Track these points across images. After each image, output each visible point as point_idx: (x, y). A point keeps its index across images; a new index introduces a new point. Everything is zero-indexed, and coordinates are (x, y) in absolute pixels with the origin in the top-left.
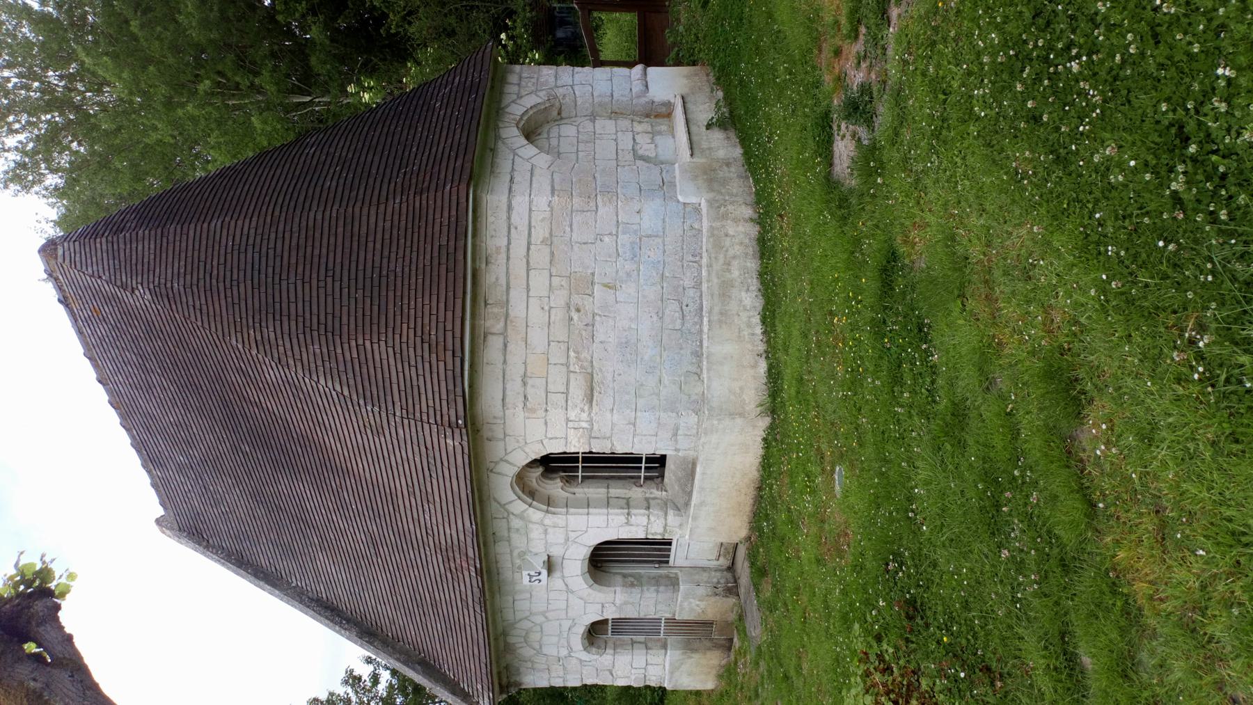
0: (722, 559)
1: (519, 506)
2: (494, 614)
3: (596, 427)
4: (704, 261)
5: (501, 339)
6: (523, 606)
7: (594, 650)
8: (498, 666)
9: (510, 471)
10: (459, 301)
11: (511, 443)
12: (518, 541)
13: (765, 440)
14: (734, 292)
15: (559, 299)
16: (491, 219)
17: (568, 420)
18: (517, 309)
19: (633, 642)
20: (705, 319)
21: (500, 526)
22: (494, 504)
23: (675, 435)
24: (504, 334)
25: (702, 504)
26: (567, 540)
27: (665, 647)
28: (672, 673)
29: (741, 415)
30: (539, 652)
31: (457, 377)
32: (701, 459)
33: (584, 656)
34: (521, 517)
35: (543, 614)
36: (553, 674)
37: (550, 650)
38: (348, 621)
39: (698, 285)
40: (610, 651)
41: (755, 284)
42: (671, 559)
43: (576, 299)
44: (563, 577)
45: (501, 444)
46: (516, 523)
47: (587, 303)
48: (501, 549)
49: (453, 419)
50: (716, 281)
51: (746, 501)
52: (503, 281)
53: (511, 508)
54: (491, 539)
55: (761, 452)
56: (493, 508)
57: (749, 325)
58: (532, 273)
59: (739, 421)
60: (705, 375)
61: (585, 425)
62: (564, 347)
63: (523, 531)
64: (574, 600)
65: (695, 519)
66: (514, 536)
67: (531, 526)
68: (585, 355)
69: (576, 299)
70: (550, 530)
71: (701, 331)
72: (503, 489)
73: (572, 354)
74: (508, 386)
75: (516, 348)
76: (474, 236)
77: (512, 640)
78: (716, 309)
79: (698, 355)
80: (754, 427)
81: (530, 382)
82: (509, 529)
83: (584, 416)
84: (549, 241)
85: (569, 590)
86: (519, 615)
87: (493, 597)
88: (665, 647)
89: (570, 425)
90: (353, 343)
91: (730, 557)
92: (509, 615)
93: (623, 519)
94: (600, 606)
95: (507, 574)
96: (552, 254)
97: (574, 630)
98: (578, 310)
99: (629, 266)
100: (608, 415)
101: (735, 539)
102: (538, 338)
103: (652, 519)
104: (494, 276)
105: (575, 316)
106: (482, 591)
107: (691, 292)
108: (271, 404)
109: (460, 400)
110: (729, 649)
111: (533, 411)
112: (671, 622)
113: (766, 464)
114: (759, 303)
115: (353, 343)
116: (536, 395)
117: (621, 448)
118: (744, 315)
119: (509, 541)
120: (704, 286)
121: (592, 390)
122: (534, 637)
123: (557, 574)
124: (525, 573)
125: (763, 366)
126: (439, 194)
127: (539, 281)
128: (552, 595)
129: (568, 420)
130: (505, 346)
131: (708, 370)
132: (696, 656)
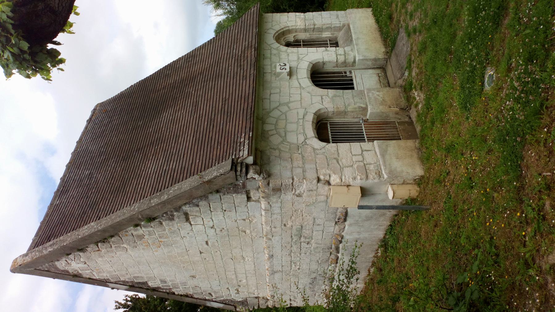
9: (272, 32)
11: (274, 23)
25: (358, 38)
26: (298, 58)
30: (284, 139)
32: (350, 22)
33: (317, 144)
34: (277, 49)
35: (287, 104)
36: (295, 164)
37: (292, 138)
44: (298, 79)
45: (271, 24)
46: (274, 52)
48: (267, 62)
51: (377, 35)
53: (272, 46)
64: (305, 94)
65: (357, 45)
66: (273, 57)
67: (281, 53)
70: (290, 55)
72: (270, 39)
77: (267, 127)
82: (271, 54)
85: (301, 87)
86: (273, 105)
87: (259, 86)
92: (267, 105)
94: (320, 98)
97: (307, 118)
119: (271, 59)
123: (294, 77)
128: (292, 91)
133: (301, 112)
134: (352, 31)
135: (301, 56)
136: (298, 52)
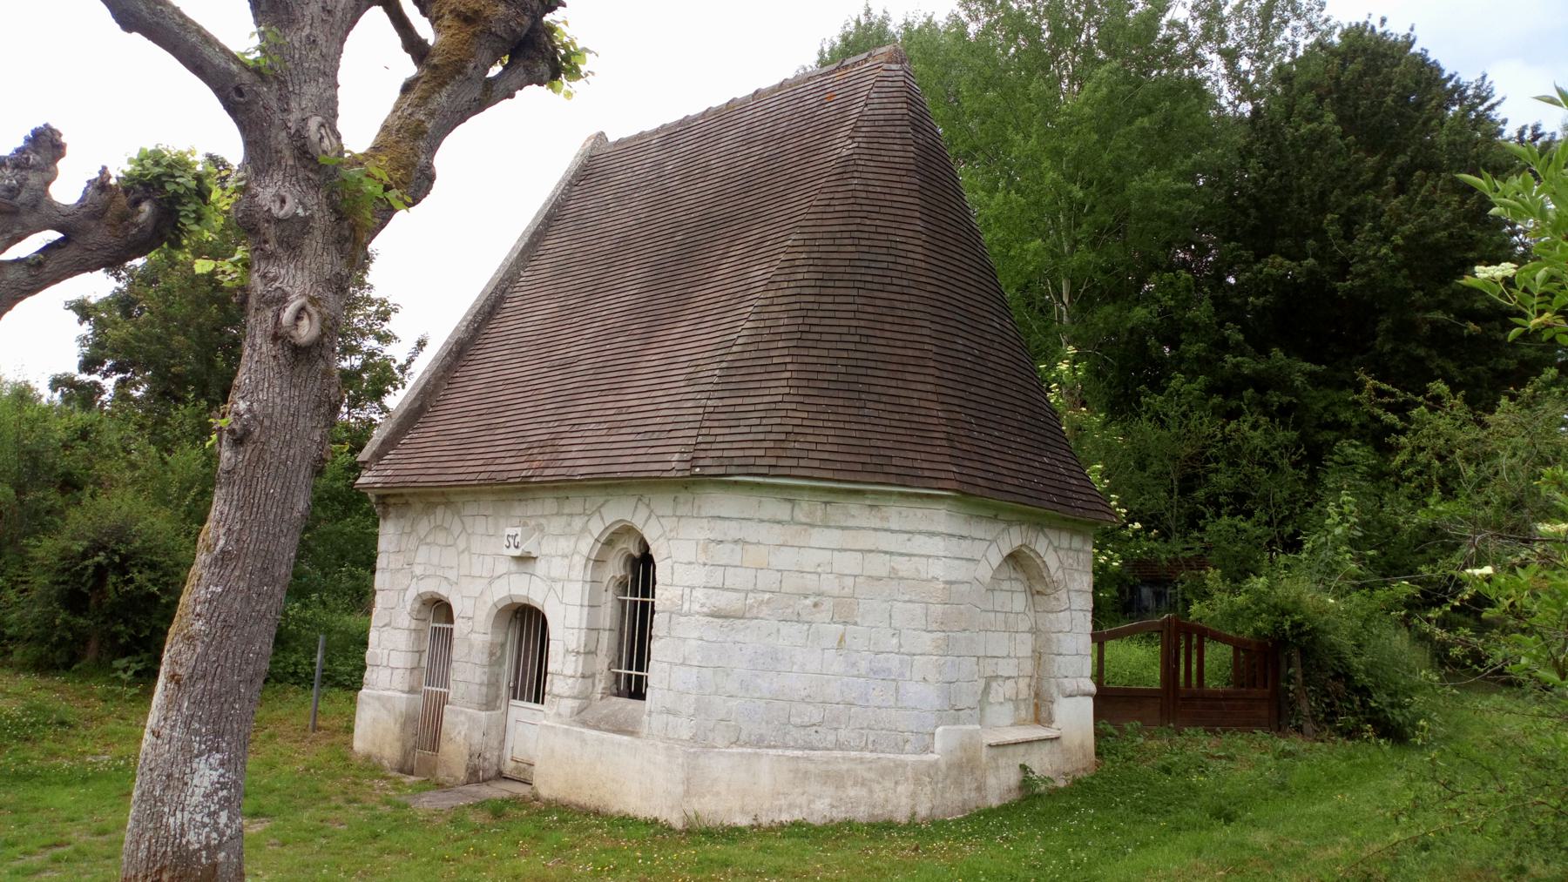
0: (513, 764)
1: (597, 527)
2: (475, 492)
3: (683, 619)
4: (868, 755)
5: (787, 517)
6: (480, 525)
7: (417, 606)
8: (411, 495)
9: (638, 521)
10: (829, 475)
11: (668, 523)
12: (556, 525)
13: (656, 820)
14: (830, 790)
15: (829, 584)
16: (919, 513)
17: (692, 588)
18: (819, 537)
19: (420, 652)
20: (799, 753)
21: (575, 505)
22: (601, 500)
23: (669, 712)
24: (793, 521)
25: (584, 741)
26: (554, 580)
27: (412, 691)
28: (379, 698)
29: (687, 793)
30: (422, 541)
31: (747, 468)
32: (638, 742)
33: (411, 594)
34: (585, 530)
35: (468, 549)
36: (392, 557)
37: (423, 554)
38: (476, 330)
39: (839, 746)
40: (414, 624)
41: (839, 815)
42: (517, 702)
43: (828, 604)
44: (509, 573)
45: (669, 512)
46: (578, 523)
47: (823, 616)
48: (549, 505)
49: (701, 462)
50: (845, 767)
51: (584, 797)
52: (851, 523)
53: (596, 518)
54: (562, 494)
55: (642, 815)
56: (597, 499)
57: (790, 806)
58: (859, 555)
59: (680, 789)
60: (735, 750)
61: (686, 607)
62: (775, 587)
63: (568, 530)
64: (479, 585)
65: (566, 732)
66: (563, 520)
67: (573, 540)
68: (765, 611)
69: (828, 604)
70: (566, 561)
71: (786, 747)
72: (619, 510)
73: (767, 596)
74: (734, 524)
75: (775, 534)
76: (901, 494)
77: (440, 511)
78: (811, 767)
79: (760, 742)
80: (672, 808)
81: (738, 548)
82: (571, 515)
83: (696, 607)
84: (894, 576)
87: (493, 493)
88: (412, 691)
89: (687, 591)
90: (788, 359)
91: (515, 775)
92: (470, 509)
93: (573, 646)
95: (518, 510)
96: (880, 579)
97: (445, 583)
98: (815, 605)
99: (863, 666)
100: (696, 634)
101: (537, 782)
102: (786, 558)
103: (570, 681)
104: (856, 512)
105: (808, 602)
106: (504, 482)
107: (831, 737)
108: (725, 269)
109: (722, 471)
110: (401, 771)
111: (705, 550)
112: (443, 700)
113: (626, 822)
114: (816, 820)
115: (788, 359)
116: (724, 554)
117: (656, 647)
118: (803, 800)
120: (838, 754)
121: (725, 617)
122: (441, 537)
123: (513, 567)
124: (519, 530)
125: (743, 821)
126: (947, 459)
127: (849, 563)
128: (489, 560)
129: (692, 588)
130: (779, 522)
131: (741, 754)
132: (396, 729)
133: (452, 575)
134: (617, 737)
135: (558, 587)
136: (570, 580)
